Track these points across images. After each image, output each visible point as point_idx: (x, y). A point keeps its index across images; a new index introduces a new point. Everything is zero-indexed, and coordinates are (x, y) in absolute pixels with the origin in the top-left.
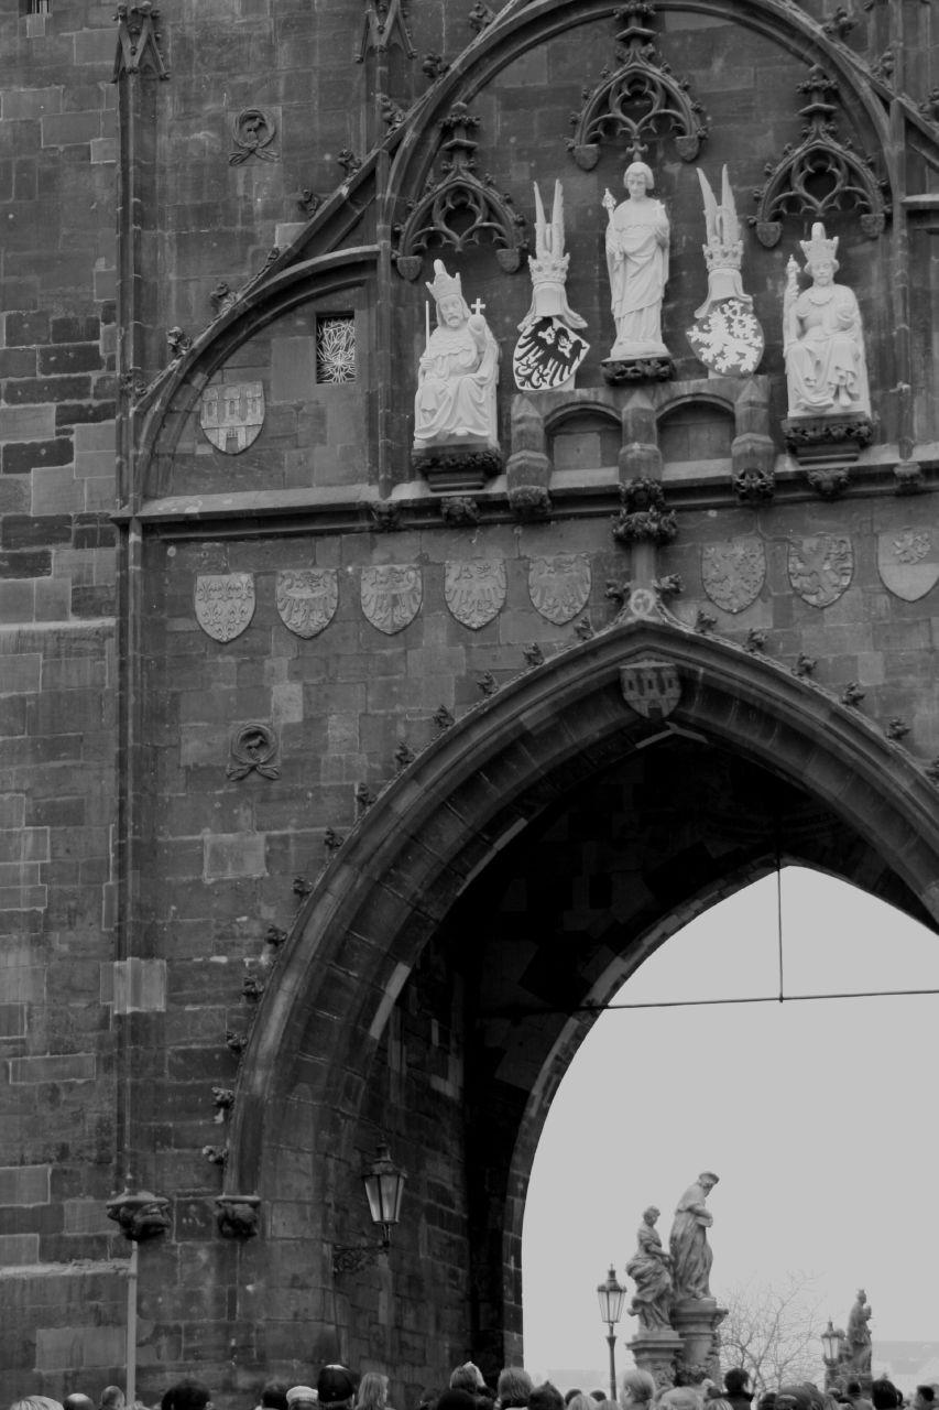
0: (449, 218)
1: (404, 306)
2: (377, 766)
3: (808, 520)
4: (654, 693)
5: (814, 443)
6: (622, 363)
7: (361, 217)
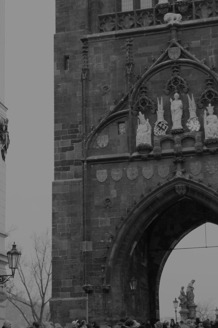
0: (142, 104)
2: (130, 205)
4: (181, 191)
5: (210, 144)
7: (126, 105)
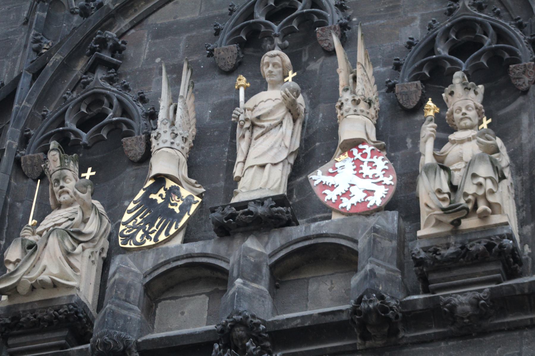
1: (22, 202)
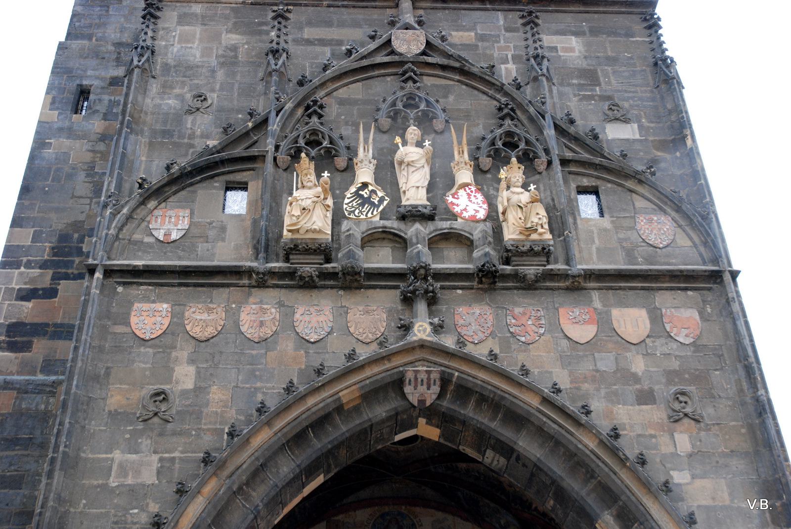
2: (242, 418)
3: (516, 298)
4: (422, 389)
5: (522, 254)
6: (410, 205)
7: (256, 142)
